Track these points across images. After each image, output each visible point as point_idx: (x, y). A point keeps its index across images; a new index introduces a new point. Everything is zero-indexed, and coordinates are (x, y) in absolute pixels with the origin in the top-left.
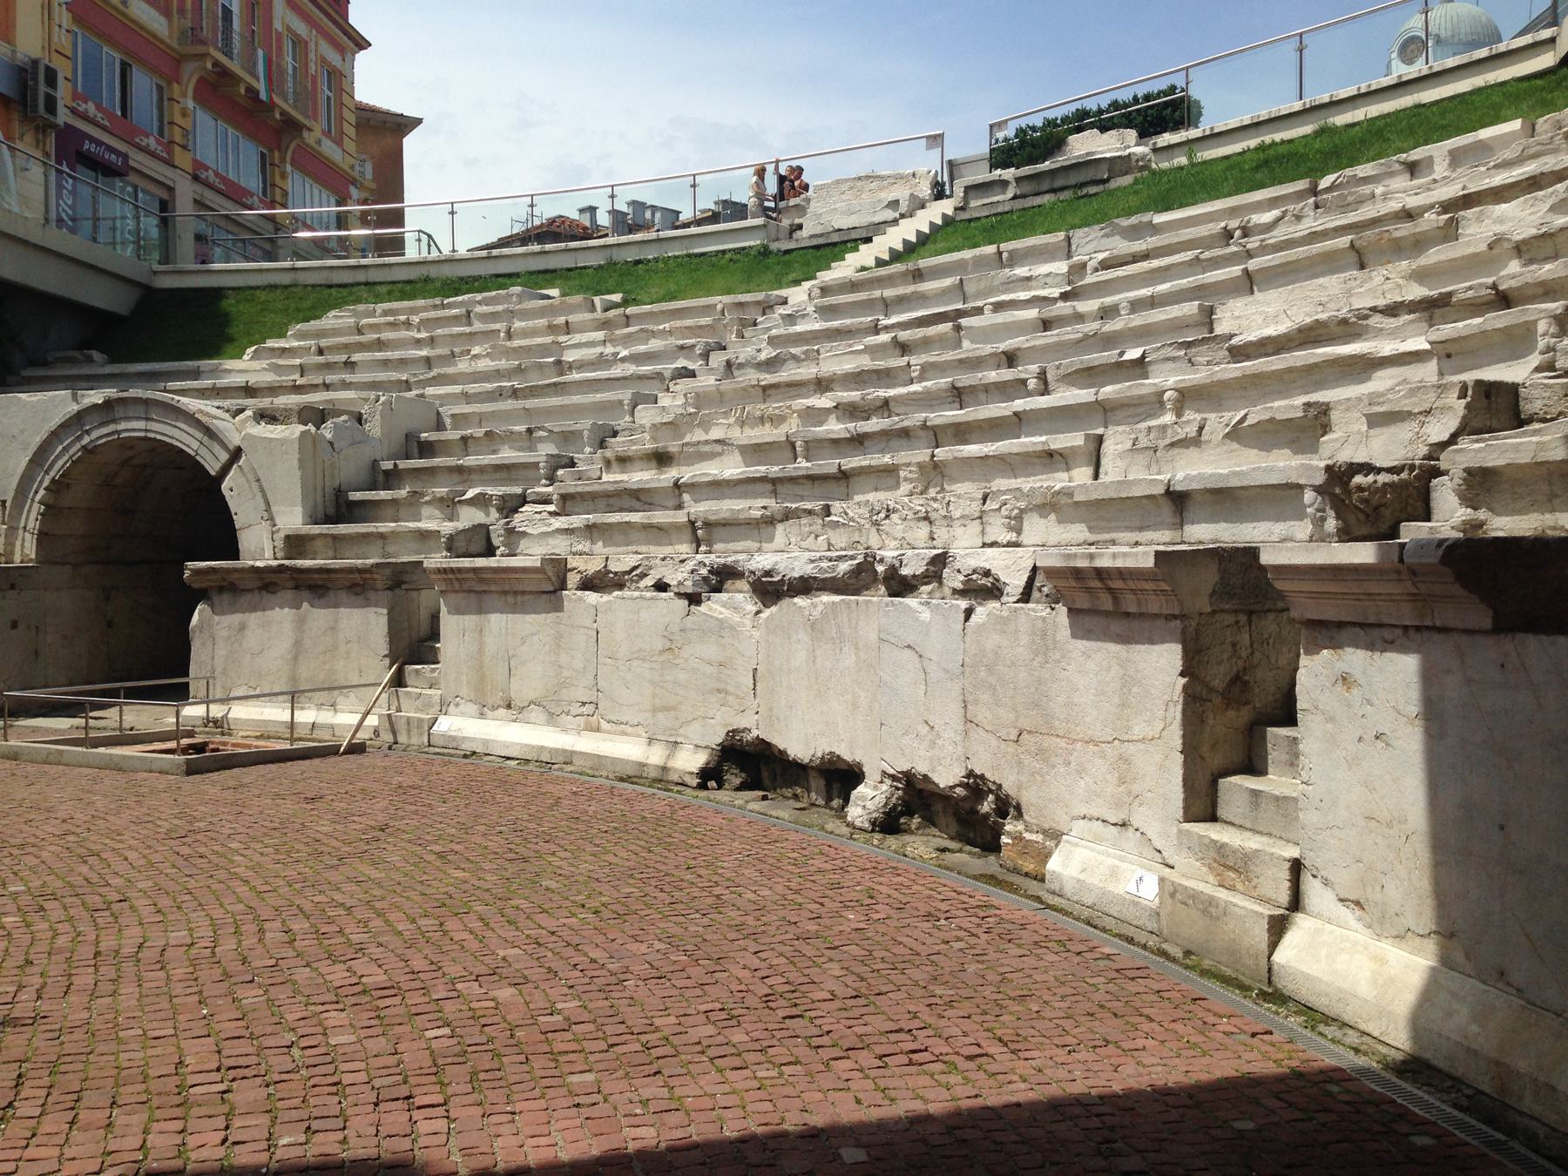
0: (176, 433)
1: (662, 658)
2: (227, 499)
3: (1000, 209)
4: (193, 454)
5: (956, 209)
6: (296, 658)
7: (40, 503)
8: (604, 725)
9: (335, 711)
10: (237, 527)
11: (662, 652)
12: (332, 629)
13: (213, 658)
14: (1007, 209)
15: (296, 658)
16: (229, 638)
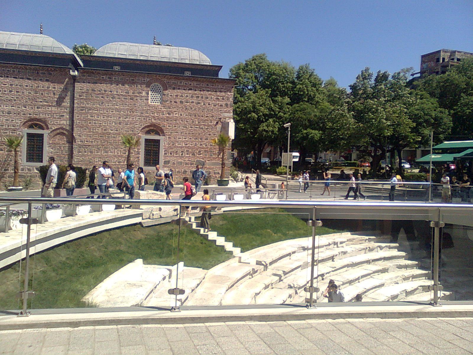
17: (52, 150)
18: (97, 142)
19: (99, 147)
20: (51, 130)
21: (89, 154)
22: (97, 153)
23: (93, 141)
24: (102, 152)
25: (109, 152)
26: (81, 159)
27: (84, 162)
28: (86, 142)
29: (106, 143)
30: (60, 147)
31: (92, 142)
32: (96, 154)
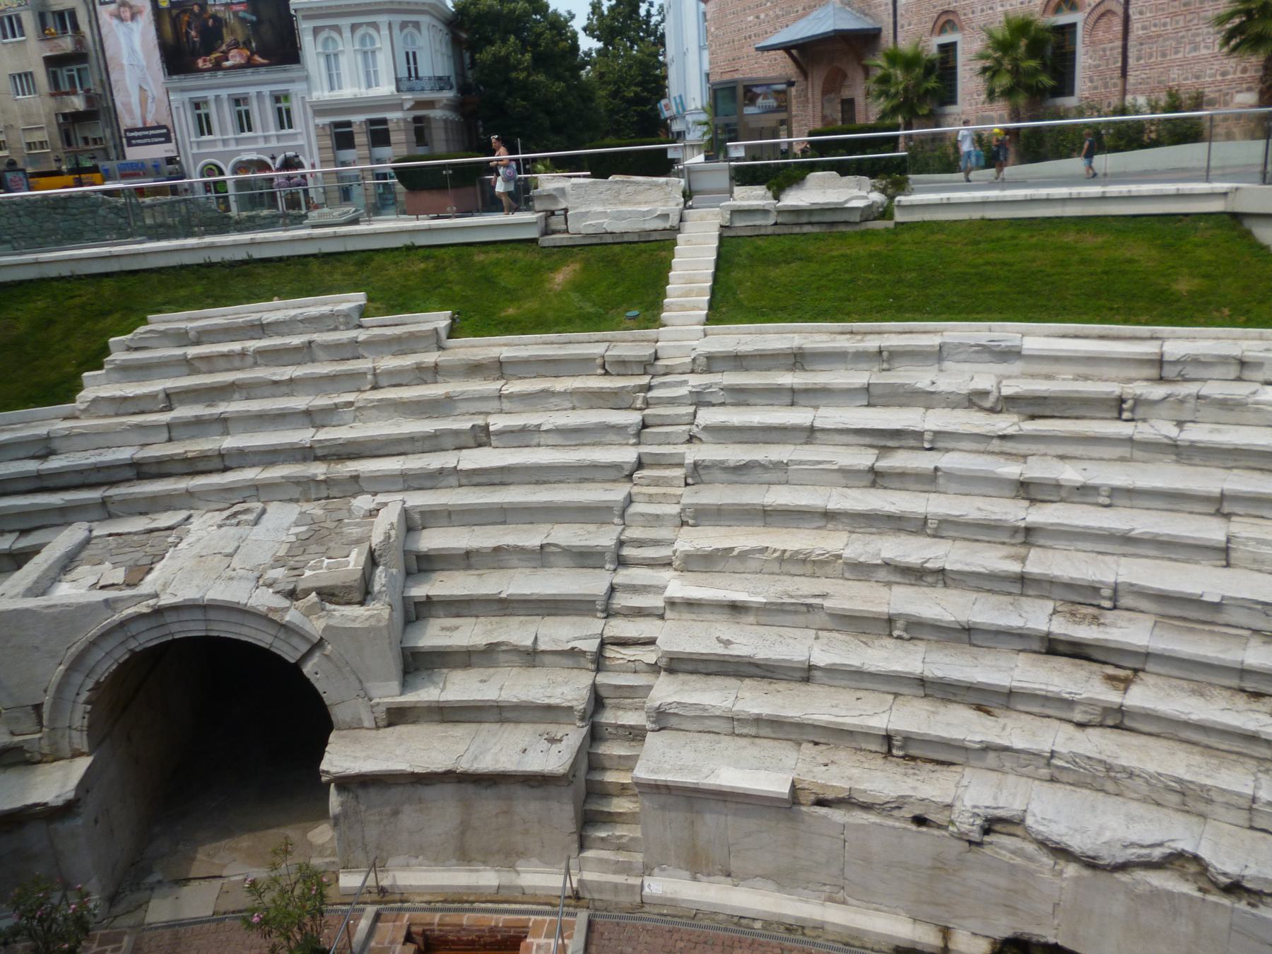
0: (253, 633)
1: (930, 872)
2: (313, 680)
3: (763, 231)
4: (267, 647)
5: (721, 226)
6: (463, 833)
7: (87, 702)
8: (849, 900)
9: (518, 872)
10: (327, 703)
11: (934, 868)
12: (505, 812)
13: (363, 838)
14: (769, 231)
15: (463, 833)
16: (381, 821)
17: (1090, 61)
18: (1177, 22)
19: (1180, 34)
20: (1088, 10)
21: (1159, 59)
22: (1176, 53)
23: (1168, 20)
24: (1187, 50)
25: (1202, 45)
26: (1143, 76)
27: (1147, 84)
28: (1153, 29)
29: (1195, 22)
30: (1104, 50)
31: (1165, 25)
32: (1174, 57)
